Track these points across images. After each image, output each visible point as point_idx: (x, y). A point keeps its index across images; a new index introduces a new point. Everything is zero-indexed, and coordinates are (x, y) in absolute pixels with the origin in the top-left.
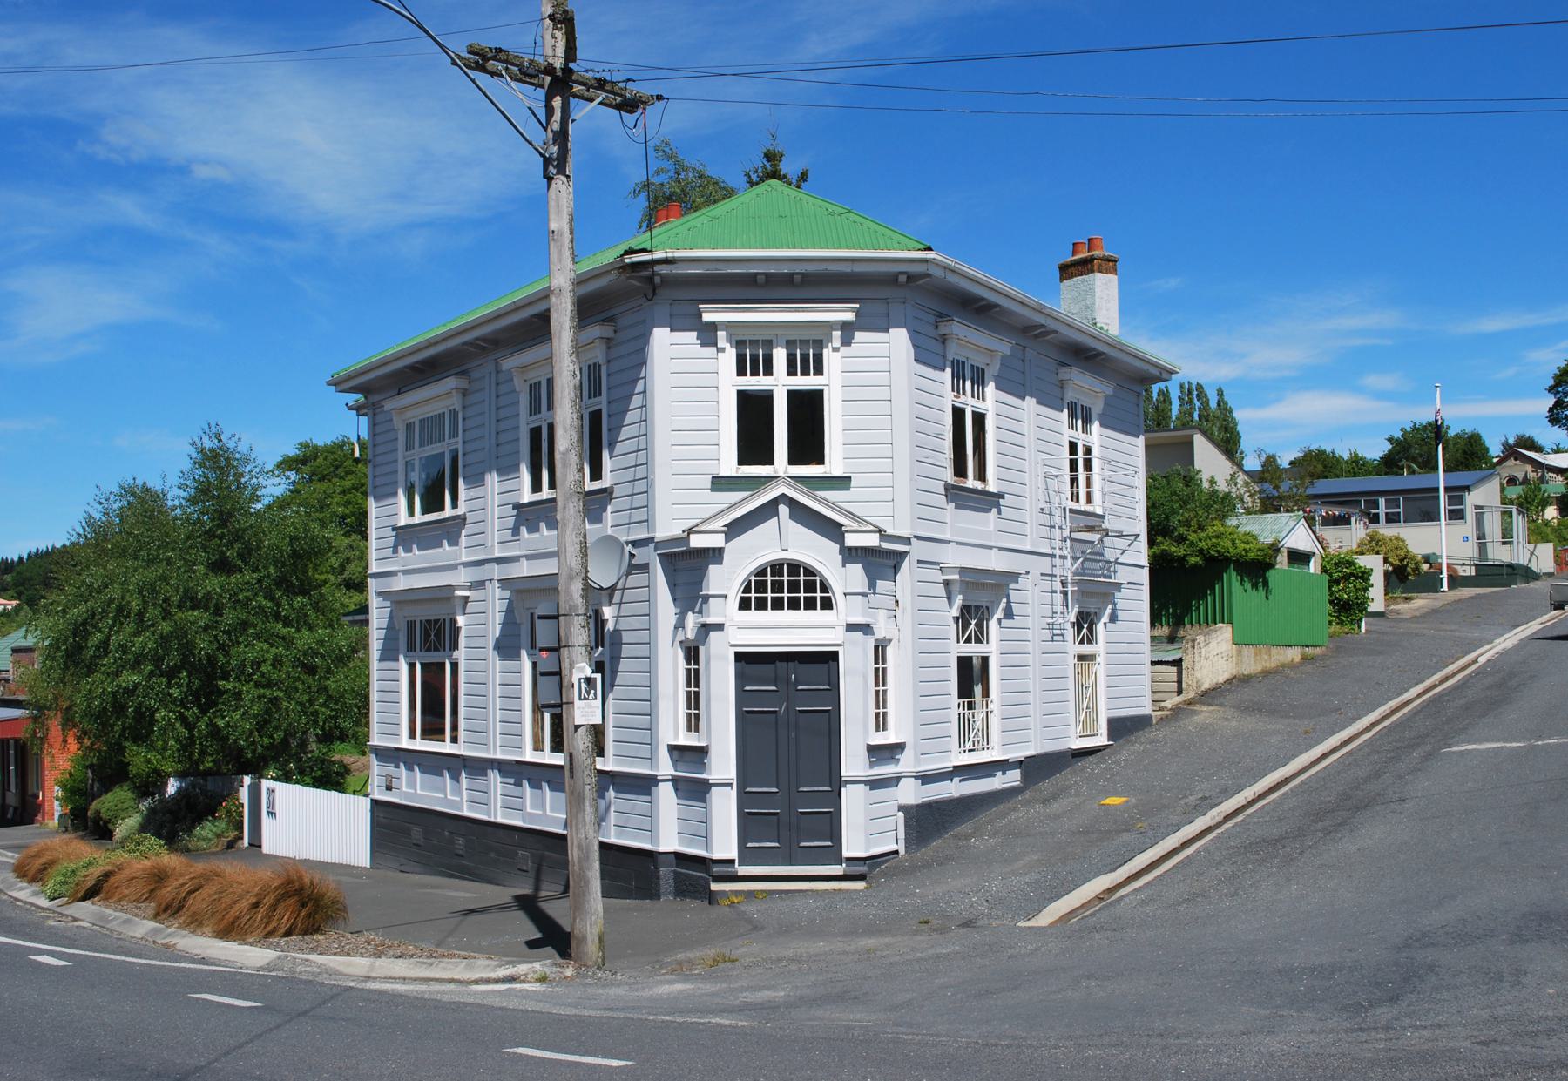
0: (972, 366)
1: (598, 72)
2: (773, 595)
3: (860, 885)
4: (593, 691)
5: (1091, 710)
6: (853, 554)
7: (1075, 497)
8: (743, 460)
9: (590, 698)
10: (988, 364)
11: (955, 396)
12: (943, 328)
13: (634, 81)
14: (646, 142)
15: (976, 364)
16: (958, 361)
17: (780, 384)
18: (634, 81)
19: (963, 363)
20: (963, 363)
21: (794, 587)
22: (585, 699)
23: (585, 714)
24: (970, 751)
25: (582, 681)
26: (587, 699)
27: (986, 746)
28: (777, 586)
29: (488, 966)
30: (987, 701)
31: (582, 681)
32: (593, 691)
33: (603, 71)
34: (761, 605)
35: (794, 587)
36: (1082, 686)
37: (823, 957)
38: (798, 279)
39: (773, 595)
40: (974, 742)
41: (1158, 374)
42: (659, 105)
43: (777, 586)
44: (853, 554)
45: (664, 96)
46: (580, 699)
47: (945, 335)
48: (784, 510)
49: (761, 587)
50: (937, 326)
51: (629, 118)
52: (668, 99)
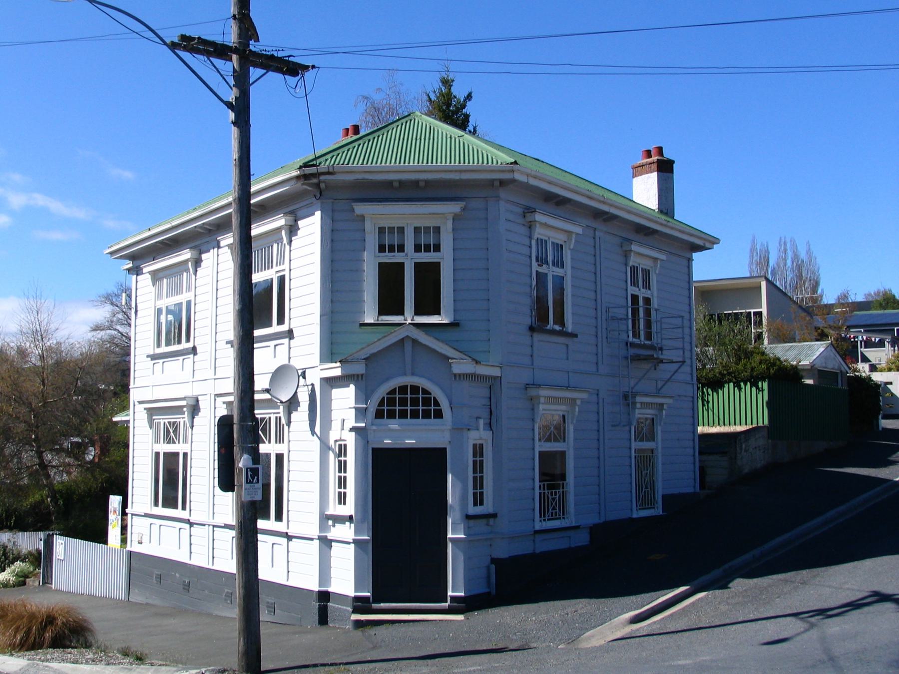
0: (553, 243)
1: (269, 51)
2: (400, 408)
3: (460, 617)
4: (256, 477)
5: (649, 490)
6: (457, 378)
7: (636, 334)
8: (382, 311)
9: (254, 482)
10: (565, 242)
11: (539, 265)
12: (529, 217)
13: (294, 57)
14: (306, 95)
15: (556, 241)
16: (542, 240)
17: (409, 259)
18: (294, 57)
19: (546, 241)
20: (546, 241)
21: (415, 402)
22: (251, 482)
23: (250, 493)
24: (548, 520)
25: (249, 470)
26: (252, 483)
27: (562, 516)
28: (403, 402)
29: (169, 671)
30: (563, 484)
31: (249, 470)
32: (256, 477)
33: (272, 50)
34: (391, 415)
35: (415, 402)
36: (641, 472)
37: (23, 641)
38: (422, 184)
39: (400, 408)
40: (552, 513)
41: (702, 244)
42: (315, 70)
43: (403, 402)
44: (457, 378)
45: (316, 66)
46: (247, 482)
47: (530, 222)
48: (408, 347)
49: (391, 402)
50: (525, 216)
51: (291, 80)
52: (319, 68)
